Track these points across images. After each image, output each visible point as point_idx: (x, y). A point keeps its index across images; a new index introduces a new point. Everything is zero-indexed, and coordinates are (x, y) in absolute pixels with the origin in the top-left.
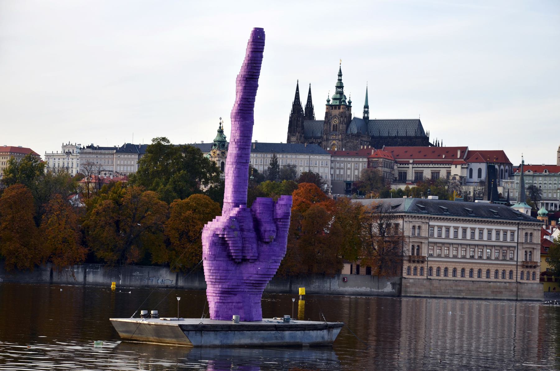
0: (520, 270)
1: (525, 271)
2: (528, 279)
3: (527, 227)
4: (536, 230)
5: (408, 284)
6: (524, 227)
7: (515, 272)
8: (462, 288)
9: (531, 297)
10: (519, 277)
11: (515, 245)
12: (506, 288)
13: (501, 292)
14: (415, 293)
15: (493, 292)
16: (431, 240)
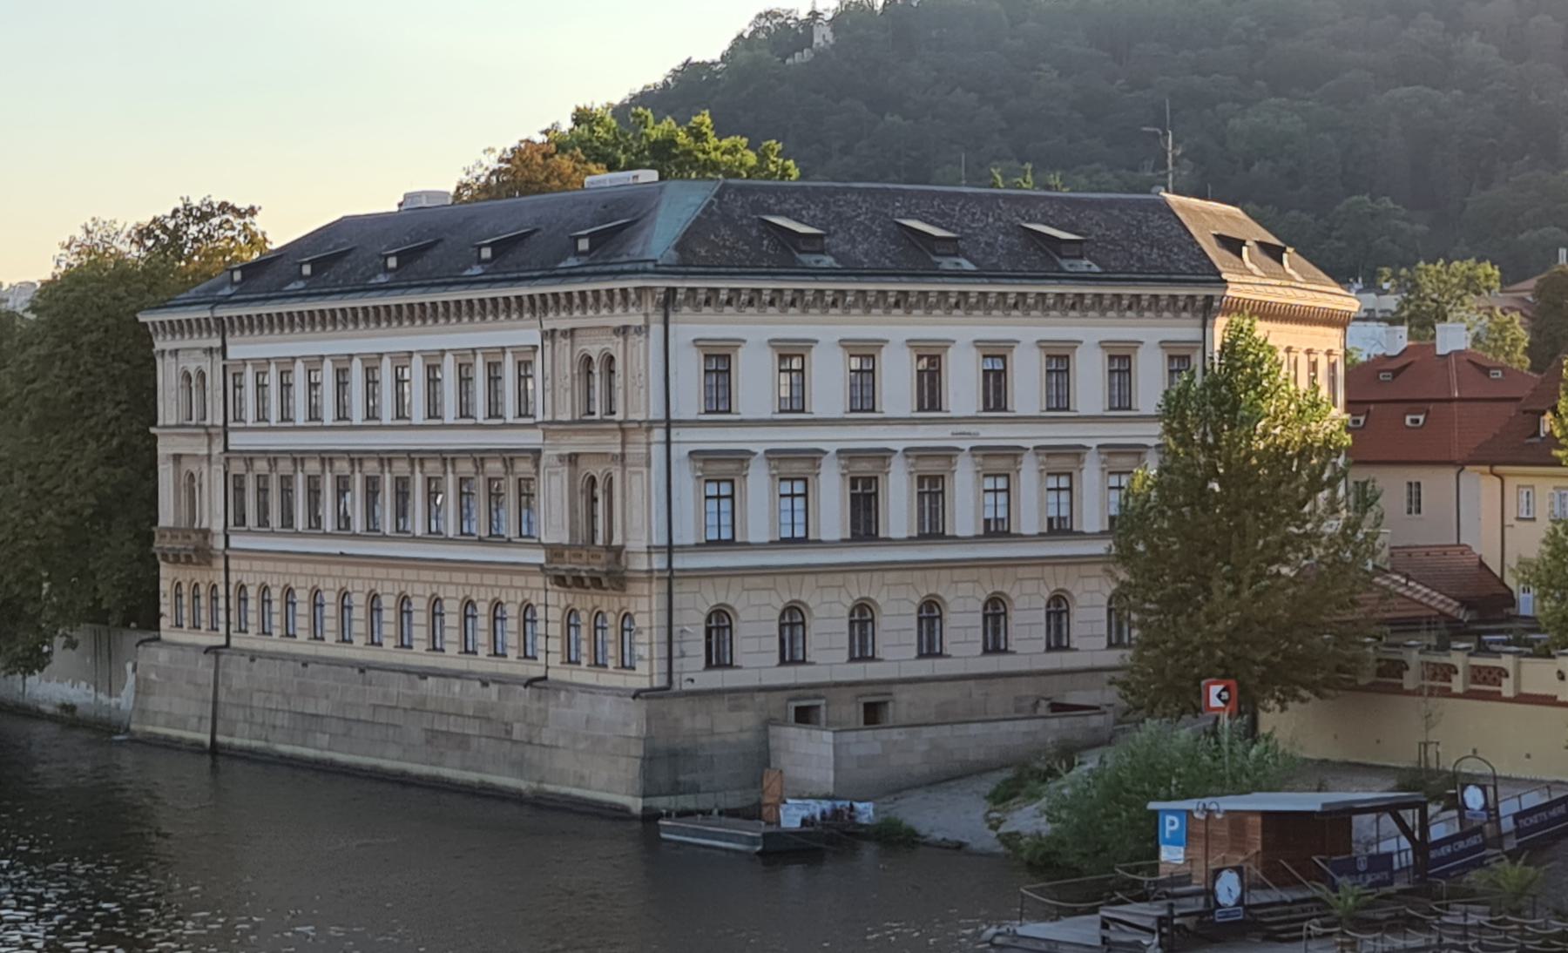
0: (558, 600)
1: (586, 602)
2: (598, 664)
3: (576, 320)
4: (616, 331)
5: (153, 676)
6: (562, 322)
7: (540, 612)
8: (323, 707)
9: (581, 781)
10: (556, 645)
11: (532, 439)
12: (482, 715)
13: (462, 741)
14: (168, 725)
15: (433, 736)
16: (237, 440)
